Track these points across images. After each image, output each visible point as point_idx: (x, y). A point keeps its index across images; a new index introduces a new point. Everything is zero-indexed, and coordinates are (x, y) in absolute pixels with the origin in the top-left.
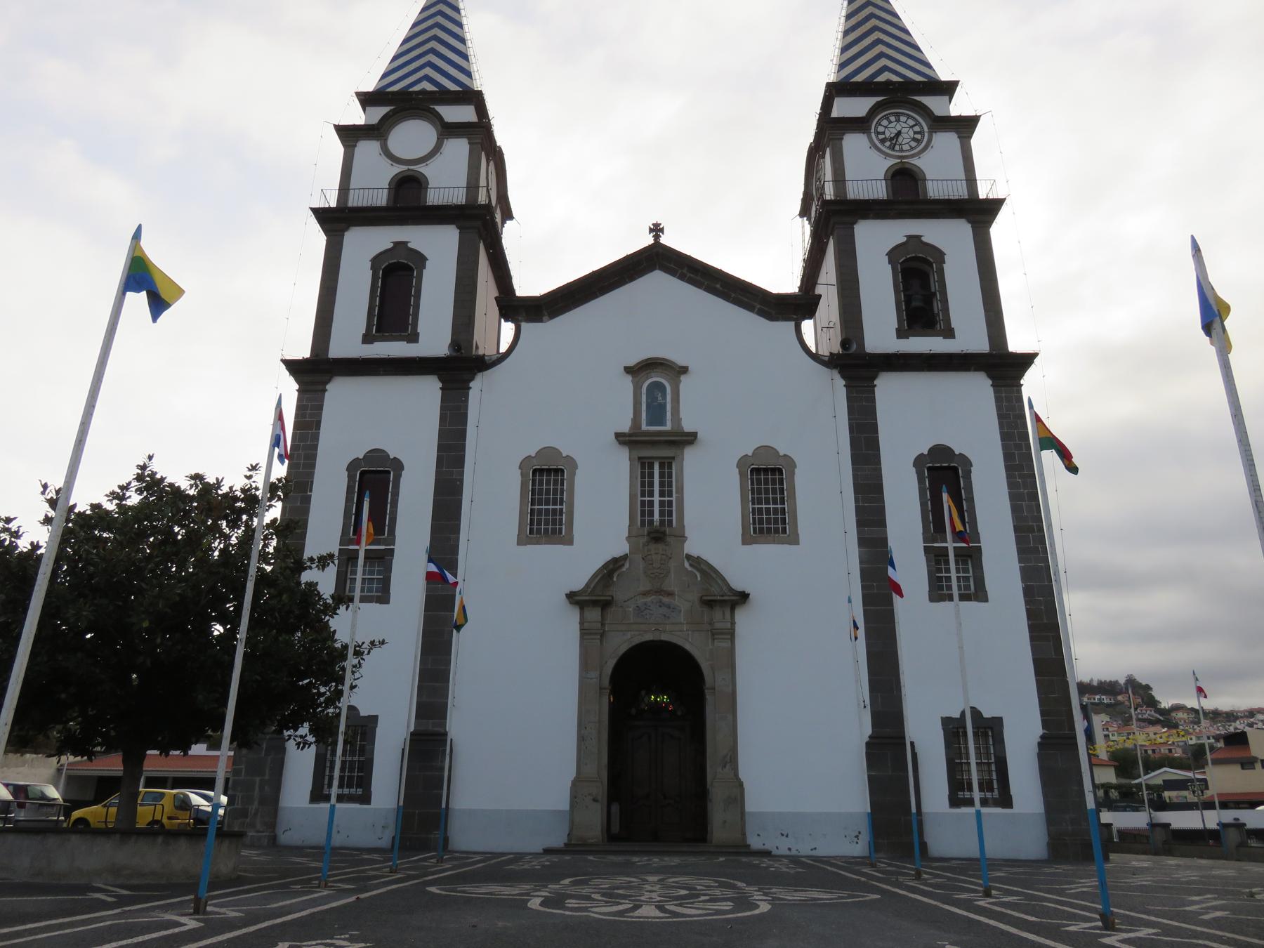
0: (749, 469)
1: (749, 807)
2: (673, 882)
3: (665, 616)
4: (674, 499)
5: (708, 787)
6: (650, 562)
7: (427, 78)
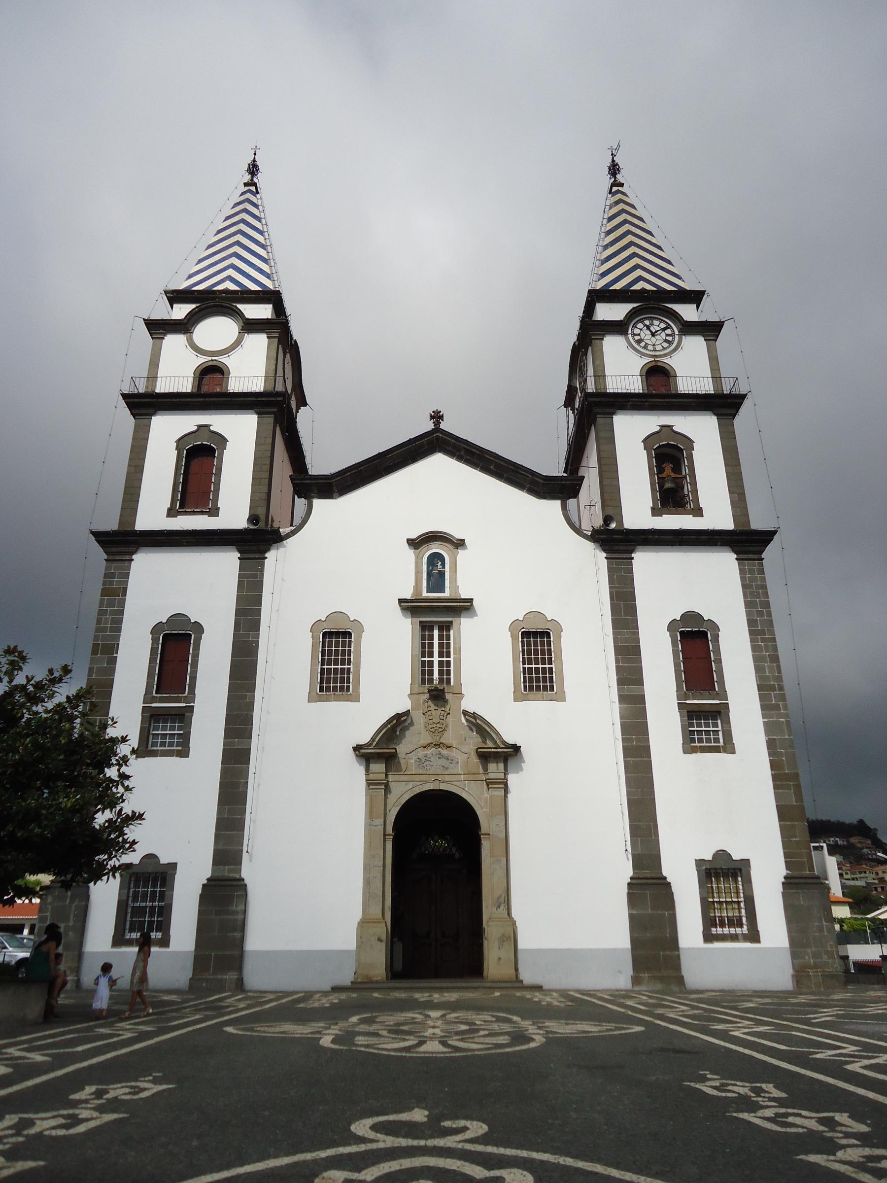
0: (520, 632)
1: (521, 945)
2: (456, 1018)
3: (443, 766)
4: (451, 659)
6: (431, 718)
7: (230, 278)
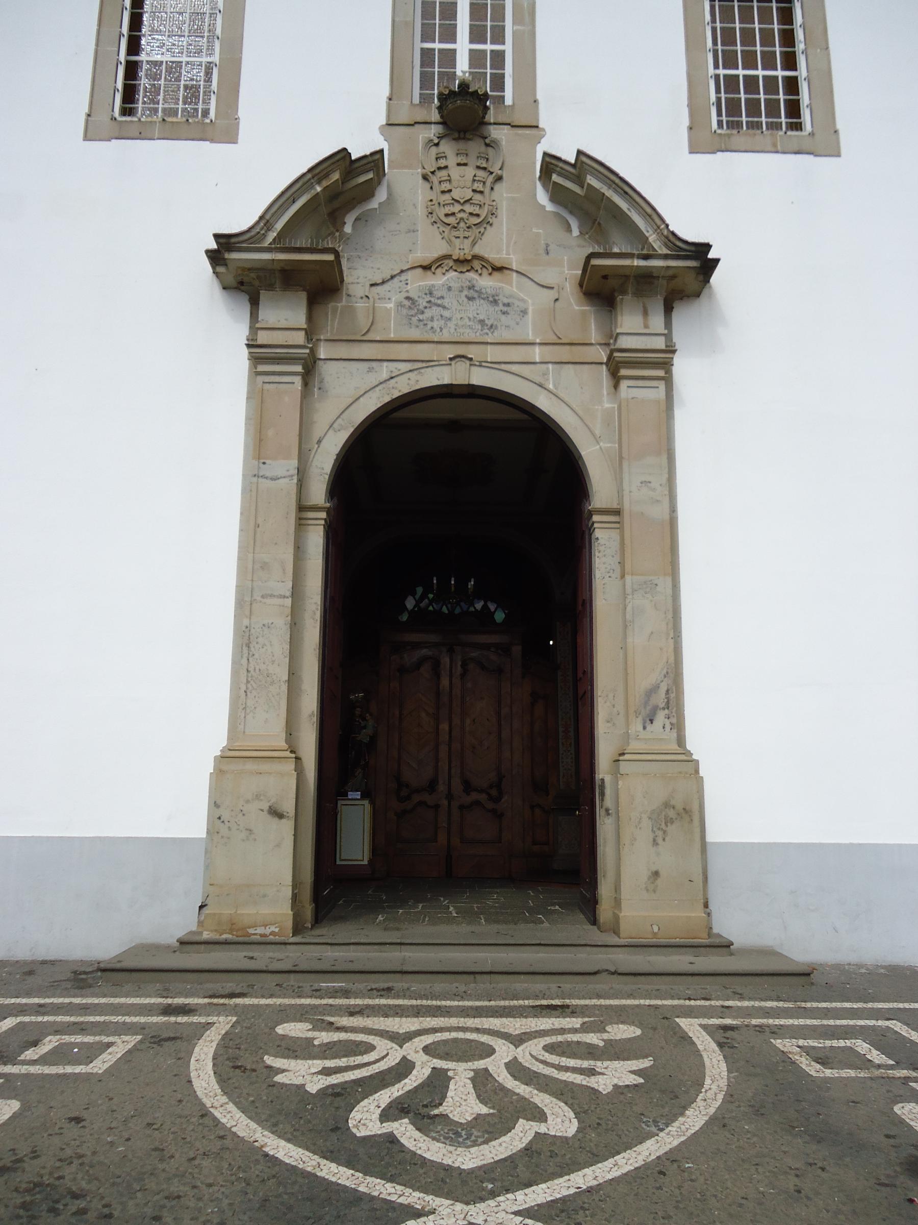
1: (711, 838)
3: (482, 322)
4: (508, 48)
5: (599, 776)
6: (446, 186)
